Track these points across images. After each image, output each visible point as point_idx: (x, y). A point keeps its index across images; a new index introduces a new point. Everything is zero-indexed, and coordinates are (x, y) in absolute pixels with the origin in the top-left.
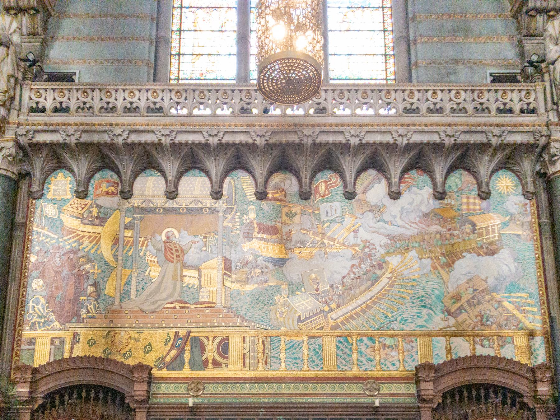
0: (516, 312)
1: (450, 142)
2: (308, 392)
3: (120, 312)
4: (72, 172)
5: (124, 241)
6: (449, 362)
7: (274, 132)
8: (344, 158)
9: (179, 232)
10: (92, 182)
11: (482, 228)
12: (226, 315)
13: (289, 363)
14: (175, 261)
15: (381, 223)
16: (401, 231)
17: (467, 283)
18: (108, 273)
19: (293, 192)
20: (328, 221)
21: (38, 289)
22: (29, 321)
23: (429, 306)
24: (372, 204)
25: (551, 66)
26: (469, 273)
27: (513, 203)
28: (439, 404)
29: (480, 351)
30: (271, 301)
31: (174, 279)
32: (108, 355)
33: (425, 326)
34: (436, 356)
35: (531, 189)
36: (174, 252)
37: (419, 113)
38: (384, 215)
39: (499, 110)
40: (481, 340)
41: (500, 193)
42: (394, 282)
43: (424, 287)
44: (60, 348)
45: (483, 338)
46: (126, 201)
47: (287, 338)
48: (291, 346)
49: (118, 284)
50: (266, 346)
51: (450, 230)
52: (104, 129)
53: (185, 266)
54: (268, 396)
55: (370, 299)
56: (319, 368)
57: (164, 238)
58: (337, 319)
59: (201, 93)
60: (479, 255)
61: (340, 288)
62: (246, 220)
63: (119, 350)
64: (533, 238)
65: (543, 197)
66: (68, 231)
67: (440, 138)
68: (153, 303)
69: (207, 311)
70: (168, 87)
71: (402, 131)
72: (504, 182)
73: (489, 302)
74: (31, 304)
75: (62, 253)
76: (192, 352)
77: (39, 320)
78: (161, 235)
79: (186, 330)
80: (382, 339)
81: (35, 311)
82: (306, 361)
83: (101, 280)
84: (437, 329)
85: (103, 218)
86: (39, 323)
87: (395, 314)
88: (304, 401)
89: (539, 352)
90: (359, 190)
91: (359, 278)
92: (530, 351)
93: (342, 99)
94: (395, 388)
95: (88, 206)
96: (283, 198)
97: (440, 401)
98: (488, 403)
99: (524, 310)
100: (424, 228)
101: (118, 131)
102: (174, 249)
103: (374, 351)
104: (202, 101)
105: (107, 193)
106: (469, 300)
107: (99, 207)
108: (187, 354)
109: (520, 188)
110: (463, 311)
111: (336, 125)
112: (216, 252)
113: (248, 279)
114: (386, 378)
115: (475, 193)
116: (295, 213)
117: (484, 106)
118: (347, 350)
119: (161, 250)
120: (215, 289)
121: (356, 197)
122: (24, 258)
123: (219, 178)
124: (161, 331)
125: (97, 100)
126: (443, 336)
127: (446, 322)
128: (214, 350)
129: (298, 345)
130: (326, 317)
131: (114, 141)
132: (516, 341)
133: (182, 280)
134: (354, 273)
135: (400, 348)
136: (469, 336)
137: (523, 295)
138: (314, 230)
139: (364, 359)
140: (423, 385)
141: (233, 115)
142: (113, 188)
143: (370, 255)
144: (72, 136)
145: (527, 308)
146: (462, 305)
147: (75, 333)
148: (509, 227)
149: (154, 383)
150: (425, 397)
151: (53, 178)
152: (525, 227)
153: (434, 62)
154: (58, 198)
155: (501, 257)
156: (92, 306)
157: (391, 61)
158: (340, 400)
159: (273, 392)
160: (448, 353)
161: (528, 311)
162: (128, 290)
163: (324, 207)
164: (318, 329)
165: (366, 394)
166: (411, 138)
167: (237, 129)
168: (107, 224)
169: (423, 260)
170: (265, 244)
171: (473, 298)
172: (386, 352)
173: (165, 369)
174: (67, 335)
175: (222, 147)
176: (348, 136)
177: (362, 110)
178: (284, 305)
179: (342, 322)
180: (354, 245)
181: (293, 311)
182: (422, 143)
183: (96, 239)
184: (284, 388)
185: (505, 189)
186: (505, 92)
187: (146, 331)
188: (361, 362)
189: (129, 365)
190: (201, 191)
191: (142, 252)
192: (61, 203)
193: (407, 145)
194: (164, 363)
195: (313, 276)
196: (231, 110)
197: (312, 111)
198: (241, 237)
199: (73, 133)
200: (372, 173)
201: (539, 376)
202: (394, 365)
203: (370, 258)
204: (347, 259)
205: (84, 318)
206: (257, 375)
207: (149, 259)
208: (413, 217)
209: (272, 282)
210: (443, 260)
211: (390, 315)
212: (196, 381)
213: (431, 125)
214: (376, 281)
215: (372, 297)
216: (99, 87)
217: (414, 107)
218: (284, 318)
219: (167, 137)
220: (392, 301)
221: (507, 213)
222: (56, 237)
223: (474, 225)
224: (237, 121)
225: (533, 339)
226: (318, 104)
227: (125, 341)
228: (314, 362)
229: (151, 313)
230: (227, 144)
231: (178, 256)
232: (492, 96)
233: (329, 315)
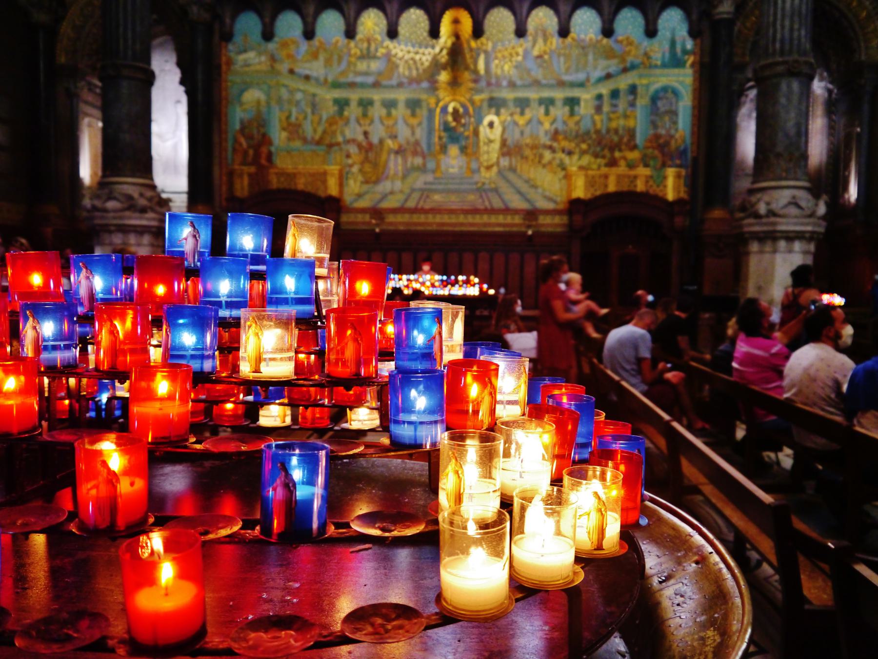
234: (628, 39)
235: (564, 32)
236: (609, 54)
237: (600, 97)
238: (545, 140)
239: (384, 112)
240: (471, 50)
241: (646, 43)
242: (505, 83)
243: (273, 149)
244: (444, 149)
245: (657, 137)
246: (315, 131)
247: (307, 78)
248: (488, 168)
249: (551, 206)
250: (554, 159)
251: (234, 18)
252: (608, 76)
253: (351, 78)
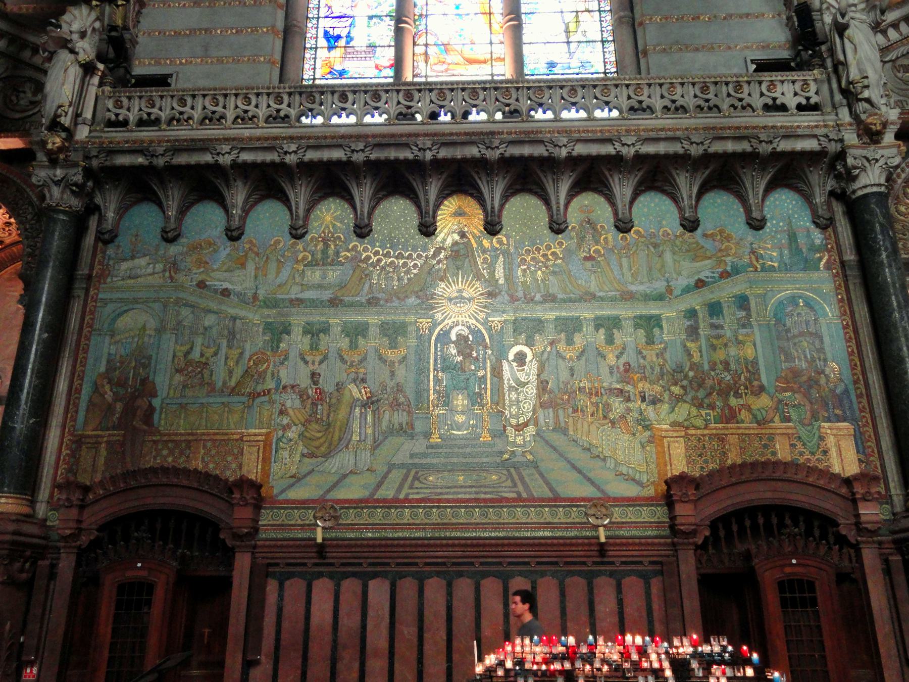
28: (706, 538)
97: (707, 533)
98: (783, 534)
141: (388, 123)
165: (589, 523)
196: (385, 116)
197: (499, 116)
201: (859, 489)
226: (508, 105)
234: (721, 232)
235: (623, 226)
236: (697, 254)
237: (692, 314)
238: (609, 381)
239: (344, 343)
240: (484, 251)
241: (750, 236)
242: (538, 297)
243: (156, 402)
244: (445, 399)
245: (796, 373)
246: (231, 372)
247: (226, 293)
248: (520, 428)
249: (632, 491)
250: (629, 410)
251: (122, 211)
252: (700, 284)
253: (294, 292)
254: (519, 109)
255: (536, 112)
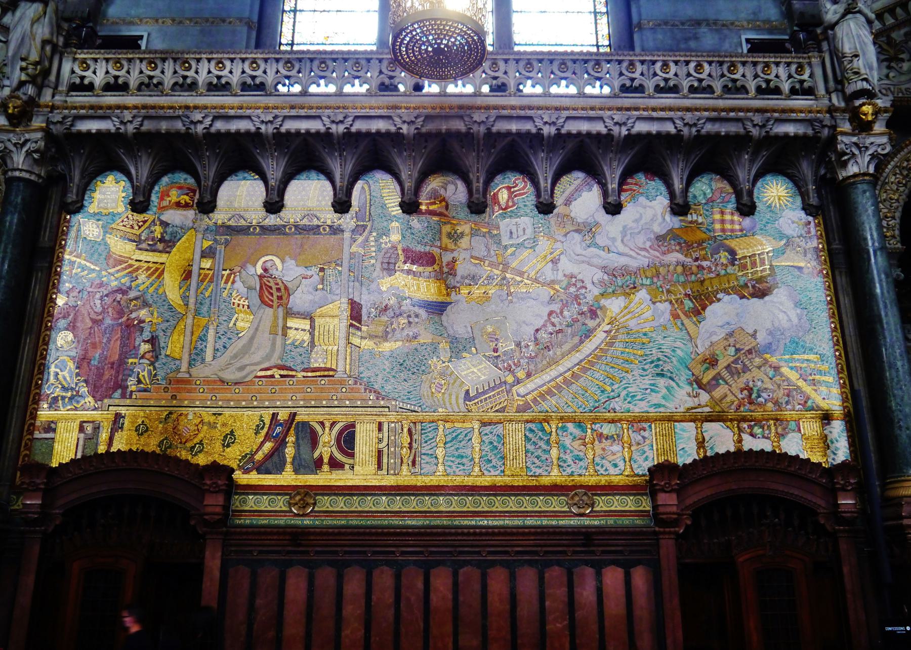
0: (801, 383)
1: (690, 133)
2: (480, 509)
3: (187, 382)
4: (128, 175)
5: (200, 275)
6: (701, 460)
7: (428, 118)
8: (535, 154)
9: (283, 261)
10: (156, 188)
11: (745, 257)
12: (352, 389)
13: (449, 463)
14: (275, 304)
15: (592, 249)
16: (623, 261)
17: (726, 339)
18: (172, 323)
19: (458, 202)
20: (512, 245)
21: (65, 346)
22: (48, 395)
23: (669, 374)
24: (579, 220)
25: (830, 32)
26: (728, 323)
27: (790, 222)
28: (687, 527)
29: (750, 444)
30: (423, 368)
31: (273, 333)
32: (166, 449)
33: (664, 406)
34: (681, 452)
35: (814, 200)
36: (274, 291)
37: (644, 93)
38: (597, 237)
39: (759, 90)
40: (750, 427)
41: (770, 206)
42: (614, 337)
43: (662, 344)
44: (92, 439)
45: (753, 423)
46: (205, 216)
47: (448, 425)
48: (454, 438)
49: (188, 339)
50: (415, 437)
51: (697, 259)
52: (177, 113)
53: (289, 313)
54: (417, 516)
55: (578, 364)
56: (497, 473)
57: (260, 271)
58: (527, 394)
59: (322, 63)
60: (742, 297)
61: (531, 348)
62: (386, 244)
63: (184, 440)
64: (821, 271)
65: (832, 212)
66: (115, 260)
67: (676, 128)
68: (242, 368)
69: (323, 382)
70: (273, 56)
71: (618, 117)
72: (775, 191)
73: (759, 368)
74: (53, 369)
75: (106, 292)
76: (297, 445)
77: (64, 394)
78: (255, 266)
79: (288, 411)
80: (598, 425)
81: (58, 379)
82: (477, 460)
83: (161, 334)
84: (682, 409)
85: (170, 241)
86: (63, 398)
87: (617, 386)
88: (473, 523)
89: (838, 445)
90: (559, 200)
91: (560, 331)
92: (826, 443)
93: (530, 72)
94: (617, 503)
95: (147, 224)
96: (444, 211)
99: (814, 380)
100: (658, 257)
101: (197, 116)
102: (274, 287)
103: (585, 444)
104: (322, 74)
105: (178, 205)
106: (729, 365)
107: (165, 224)
108: (290, 449)
109: (799, 200)
110: (720, 381)
111: (522, 108)
112: (338, 292)
113: (387, 333)
114: (603, 488)
115: (731, 206)
116: (462, 234)
117: (739, 84)
118: (542, 444)
119: (255, 289)
120: (335, 348)
121: (555, 211)
122: (47, 301)
123: (346, 183)
124: (250, 413)
125: (169, 72)
126: (691, 421)
127: (696, 399)
128: (332, 443)
129: (465, 436)
130: (508, 392)
131: (190, 131)
132: (804, 428)
133: (285, 335)
134: (554, 325)
135: (625, 439)
136: (731, 420)
137: (812, 357)
138: (491, 260)
139: (569, 458)
140: (662, 498)
141: (369, 94)
142: (187, 198)
143: (577, 297)
144: (129, 124)
145: (817, 377)
146: (719, 374)
147: (117, 414)
148: (785, 255)
149: (236, 494)
150: (664, 517)
151: (99, 183)
152: (809, 256)
153: (666, 23)
154: (104, 211)
155: (775, 300)
156: (145, 373)
157: (603, 21)
158: (530, 522)
159: (425, 509)
160: (699, 448)
161: (819, 382)
162: (201, 350)
163: (505, 225)
164: (496, 411)
165: (572, 512)
166: (632, 127)
167: (372, 113)
168: (175, 249)
169: (658, 304)
170: (415, 280)
171: (735, 362)
172: (603, 445)
173: (255, 472)
174: (104, 417)
175: (351, 139)
176: (539, 123)
177: (559, 86)
178: (442, 375)
179: (535, 400)
180: (553, 282)
181: (458, 383)
182: (649, 134)
183: (158, 272)
184: (443, 504)
185: (777, 201)
186: (767, 65)
187: (227, 412)
188: (565, 461)
189: (198, 465)
190: (318, 200)
191: (226, 291)
192: (106, 219)
193: (629, 136)
194: (253, 463)
195: (490, 329)
196: (366, 86)
197: (486, 89)
198: (378, 269)
199: (131, 119)
200: (576, 178)
202: (615, 466)
203: (576, 300)
204: (542, 303)
205: (132, 392)
206: (401, 483)
207: (236, 301)
208: (641, 240)
209: (426, 338)
210: (688, 304)
211: (609, 389)
212: (302, 490)
213: (662, 109)
214: (587, 337)
215: (581, 361)
216: (174, 56)
217: (636, 83)
218: (444, 394)
219: (269, 124)
220: (612, 367)
221: (781, 235)
222: (97, 269)
223: (733, 253)
224: (374, 101)
225: (829, 424)
226: (495, 78)
227: (193, 428)
228: (490, 461)
229: (236, 384)
230: (359, 133)
231: (280, 298)
232: (749, 71)
233: (514, 389)
254: (505, 81)
255: (525, 86)
